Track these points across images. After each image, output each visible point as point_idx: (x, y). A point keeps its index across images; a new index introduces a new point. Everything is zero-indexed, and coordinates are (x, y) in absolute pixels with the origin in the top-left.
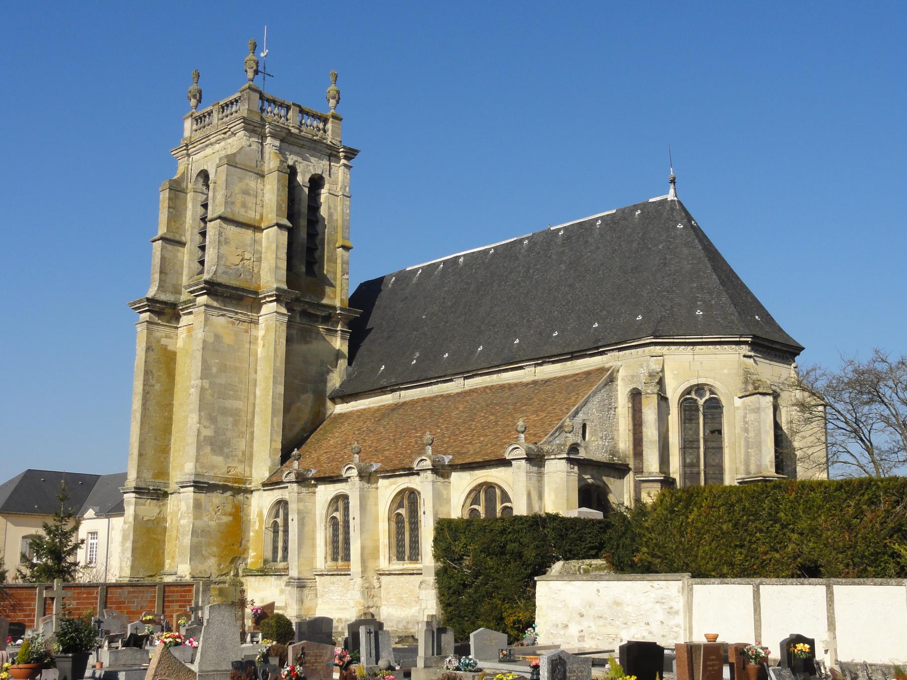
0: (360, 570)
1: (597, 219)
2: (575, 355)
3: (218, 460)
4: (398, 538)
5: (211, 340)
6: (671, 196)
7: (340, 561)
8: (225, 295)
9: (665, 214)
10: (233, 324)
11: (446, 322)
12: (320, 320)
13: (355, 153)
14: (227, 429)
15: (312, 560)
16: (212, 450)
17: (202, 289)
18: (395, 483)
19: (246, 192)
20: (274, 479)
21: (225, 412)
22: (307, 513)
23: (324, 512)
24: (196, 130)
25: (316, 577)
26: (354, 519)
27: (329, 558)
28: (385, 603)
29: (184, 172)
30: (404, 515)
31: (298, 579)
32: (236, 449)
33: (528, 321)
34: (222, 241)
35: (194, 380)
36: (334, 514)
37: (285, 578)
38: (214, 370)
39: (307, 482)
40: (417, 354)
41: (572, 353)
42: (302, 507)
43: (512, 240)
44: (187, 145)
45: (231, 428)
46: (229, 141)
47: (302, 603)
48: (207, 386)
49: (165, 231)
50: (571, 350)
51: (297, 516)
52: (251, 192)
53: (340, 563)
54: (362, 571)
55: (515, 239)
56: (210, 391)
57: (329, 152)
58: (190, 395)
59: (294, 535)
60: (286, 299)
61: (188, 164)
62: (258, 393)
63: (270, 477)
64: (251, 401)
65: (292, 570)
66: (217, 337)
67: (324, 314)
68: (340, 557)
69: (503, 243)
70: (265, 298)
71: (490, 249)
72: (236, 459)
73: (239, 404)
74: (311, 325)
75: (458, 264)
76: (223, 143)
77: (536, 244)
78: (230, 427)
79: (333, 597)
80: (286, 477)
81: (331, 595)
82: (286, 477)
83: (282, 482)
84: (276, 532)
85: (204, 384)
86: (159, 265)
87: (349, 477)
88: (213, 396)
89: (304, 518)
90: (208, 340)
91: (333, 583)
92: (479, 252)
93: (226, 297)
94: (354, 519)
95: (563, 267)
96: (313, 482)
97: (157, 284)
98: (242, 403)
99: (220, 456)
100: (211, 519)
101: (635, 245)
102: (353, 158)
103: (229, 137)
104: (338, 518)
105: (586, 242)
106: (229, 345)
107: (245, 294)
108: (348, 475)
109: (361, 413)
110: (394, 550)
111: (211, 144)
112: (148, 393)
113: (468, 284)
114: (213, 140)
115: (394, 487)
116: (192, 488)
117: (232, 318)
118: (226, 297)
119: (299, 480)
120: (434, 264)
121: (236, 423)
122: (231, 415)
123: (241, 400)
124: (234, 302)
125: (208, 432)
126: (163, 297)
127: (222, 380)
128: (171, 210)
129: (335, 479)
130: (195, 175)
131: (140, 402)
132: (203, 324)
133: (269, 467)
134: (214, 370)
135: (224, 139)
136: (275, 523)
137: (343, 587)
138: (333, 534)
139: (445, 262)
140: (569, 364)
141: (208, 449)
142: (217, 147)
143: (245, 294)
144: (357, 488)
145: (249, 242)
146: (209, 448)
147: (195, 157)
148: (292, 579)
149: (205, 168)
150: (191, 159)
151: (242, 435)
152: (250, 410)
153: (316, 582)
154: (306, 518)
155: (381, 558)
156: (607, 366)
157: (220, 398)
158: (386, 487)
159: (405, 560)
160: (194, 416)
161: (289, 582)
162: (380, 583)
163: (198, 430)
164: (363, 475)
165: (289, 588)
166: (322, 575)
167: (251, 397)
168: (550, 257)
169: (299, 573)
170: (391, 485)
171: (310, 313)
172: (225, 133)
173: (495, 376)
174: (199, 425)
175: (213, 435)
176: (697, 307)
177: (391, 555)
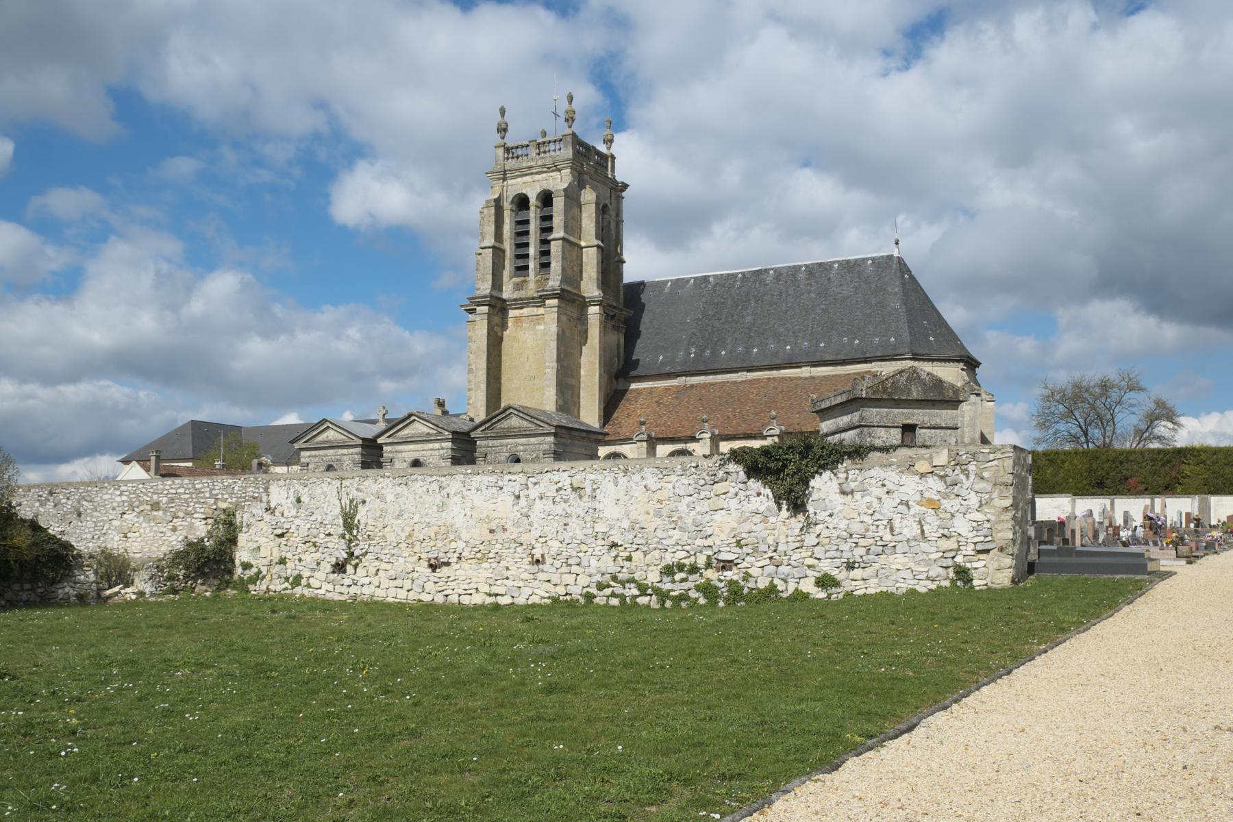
1: (834, 262)
2: (844, 362)
5: (560, 333)
6: (896, 254)
9: (894, 266)
10: (570, 320)
17: (557, 294)
19: (573, 218)
24: (508, 159)
33: (794, 333)
40: (693, 350)
41: (844, 360)
43: (758, 268)
44: (505, 171)
46: (551, 174)
49: (493, 241)
50: (843, 358)
55: (760, 268)
66: (563, 330)
69: (749, 270)
71: (738, 274)
75: (709, 281)
76: (544, 175)
77: (781, 274)
83: (632, 439)
86: (491, 268)
92: (728, 274)
95: (813, 295)
97: (490, 283)
101: (873, 286)
102: (624, 191)
103: (553, 171)
105: (829, 279)
108: (700, 437)
109: (651, 390)
111: (532, 174)
114: (534, 171)
120: (683, 279)
126: (495, 293)
130: (512, 197)
131: (485, 376)
132: (556, 320)
134: (562, 355)
135: (546, 172)
139: (696, 278)
140: (839, 367)
142: (537, 177)
145: (575, 257)
147: (510, 182)
149: (524, 192)
150: (505, 183)
156: (873, 370)
158: (724, 446)
168: (798, 286)
172: (548, 168)
173: (775, 372)
176: (930, 335)
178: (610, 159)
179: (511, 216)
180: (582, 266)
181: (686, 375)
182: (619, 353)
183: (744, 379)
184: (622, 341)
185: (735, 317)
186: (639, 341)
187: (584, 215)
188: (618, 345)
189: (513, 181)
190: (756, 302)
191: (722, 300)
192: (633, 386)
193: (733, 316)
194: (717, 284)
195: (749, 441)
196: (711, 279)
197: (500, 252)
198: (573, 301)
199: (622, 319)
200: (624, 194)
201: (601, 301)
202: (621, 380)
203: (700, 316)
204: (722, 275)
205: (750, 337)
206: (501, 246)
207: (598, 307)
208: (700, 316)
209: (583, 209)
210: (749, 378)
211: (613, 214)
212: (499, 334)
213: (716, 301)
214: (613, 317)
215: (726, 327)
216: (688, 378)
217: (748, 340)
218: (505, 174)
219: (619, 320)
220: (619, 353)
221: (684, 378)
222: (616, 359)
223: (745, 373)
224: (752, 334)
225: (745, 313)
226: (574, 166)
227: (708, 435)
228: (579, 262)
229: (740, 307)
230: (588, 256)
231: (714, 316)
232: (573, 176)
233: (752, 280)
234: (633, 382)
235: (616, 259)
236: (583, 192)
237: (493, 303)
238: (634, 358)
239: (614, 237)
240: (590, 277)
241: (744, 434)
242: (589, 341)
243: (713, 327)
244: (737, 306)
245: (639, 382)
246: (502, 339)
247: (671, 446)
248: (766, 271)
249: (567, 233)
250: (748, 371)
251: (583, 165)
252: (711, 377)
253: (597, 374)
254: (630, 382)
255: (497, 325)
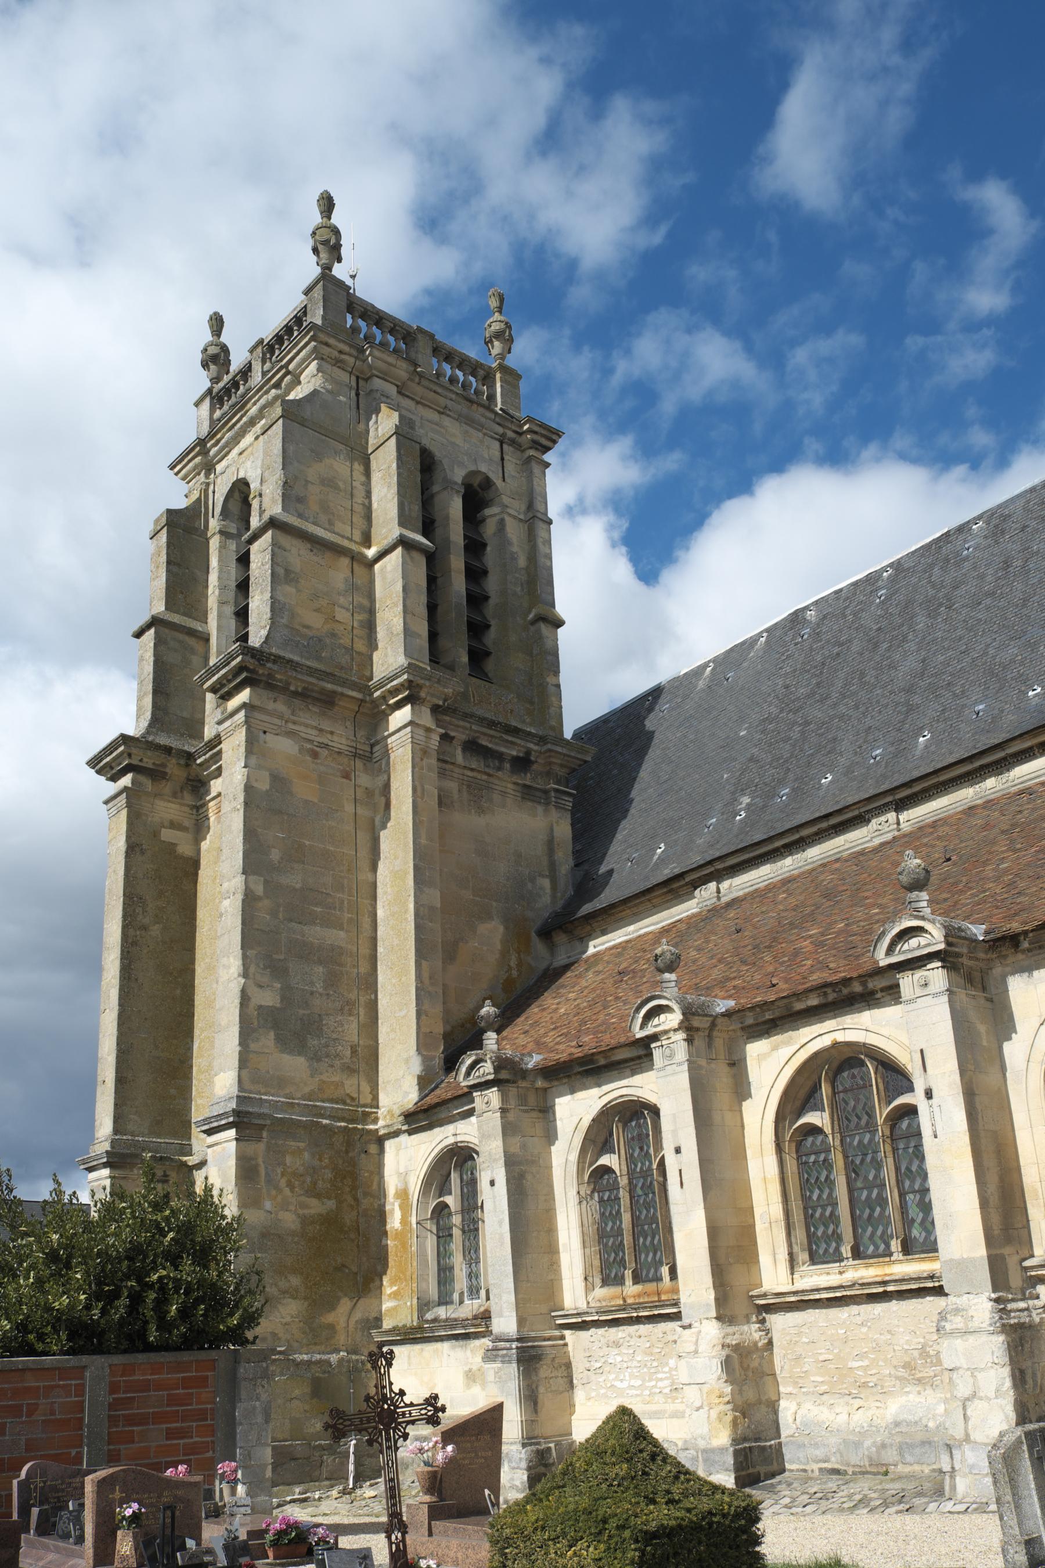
0: (712, 1295)
3: (295, 1065)
4: (806, 1200)
7: (629, 1281)
8: (292, 688)
10: (315, 755)
11: (807, 723)
12: (507, 766)
13: (554, 437)
14: (312, 993)
15: (551, 1289)
16: (278, 1039)
17: (241, 669)
18: (788, 1043)
20: (431, 1100)
21: (306, 952)
22: (533, 1162)
23: (574, 1156)
25: (567, 1333)
26: (678, 1151)
27: (598, 1281)
28: (789, 1389)
29: (199, 499)
30: (828, 1130)
31: (518, 1340)
32: (335, 1040)
34: (281, 575)
35: (229, 880)
36: (605, 1160)
37: (486, 1342)
38: (275, 855)
39: (523, 1084)
40: (746, 800)
42: (515, 1149)
45: (321, 990)
47: (536, 1403)
48: (259, 889)
49: (163, 608)
51: (503, 1170)
52: (341, 484)
53: (631, 1289)
54: (717, 1299)
56: (266, 903)
57: (500, 430)
58: (221, 915)
59: (500, 1223)
60: (433, 695)
61: (208, 484)
62: (380, 913)
63: (421, 1100)
64: (366, 932)
65: (501, 1315)
66: (277, 779)
67: (514, 753)
68: (628, 1274)
70: (383, 698)
72: (337, 1063)
73: (337, 937)
74: (489, 775)
78: (319, 987)
79: (618, 1384)
80: (468, 1074)
81: (612, 1377)
82: (468, 1074)
84: (444, 1236)
85: (252, 886)
87: (655, 1037)
88: (274, 914)
89: (522, 1176)
90: (255, 784)
91: (617, 1345)
93: (296, 694)
94: (678, 1151)
96: (540, 1083)
98: (342, 934)
99: (299, 1054)
100: (284, 1206)
102: (548, 449)
104: (616, 1167)
106: (306, 802)
107: (339, 689)
110: (800, 1234)
112: (134, 943)
113: (841, 645)
115: (786, 1052)
116: (232, 1133)
117: (311, 741)
118: (296, 694)
119: (504, 1075)
121: (333, 980)
122: (320, 962)
123: (342, 929)
124: (315, 709)
125: (268, 998)
127: (294, 880)
128: (175, 569)
129: (602, 1062)
130: (222, 499)
133: (419, 1078)
134: (275, 855)
136: (441, 1209)
137: (648, 1352)
138: (602, 1215)
141: (267, 1041)
143: (339, 689)
144: (680, 1064)
146: (272, 1034)
148: (501, 1340)
149: (241, 475)
151: (348, 1007)
152: (364, 950)
153: (566, 1345)
154: (529, 1177)
155: (765, 1258)
157: (291, 920)
158: (761, 1058)
159: (841, 1260)
160: (232, 960)
161: (495, 1349)
162: (768, 1331)
163: (243, 991)
164: (696, 1022)
165: (492, 1367)
166: (583, 1326)
167: (366, 921)
169: (521, 1322)
170: (775, 1048)
171: (483, 746)
174: (243, 981)
175: (278, 1005)
177: (796, 1249)
178: (498, 376)
179: (222, 547)
180: (372, 612)
181: (718, 876)
182: (553, 866)
183: (889, 837)
184: (564, 829)
185: (869, 678)
186: (624, 824)
187: (376, 477)
188: (550, 844)
189: (224, 463)
190: (933, 614)
191: (836, 650)
192: (596, 946)
193: (863, 675)
194: (825, 617)
195: (848, 1020)
196: (811, 615)
197: (191, 641)
198: (327, 701)
199: (562, 772)
200: (548, 457)
201: (409, 684)
202: (560, 938)
203: (774, 710)
204: (841, 590)
205: (911, 709)
206: (198, 626)
207: (408, 708)
208: (774, 710)
209: (374, 465)
210: (905, 827)
211: (516, 507)
212: (185, 849)
213: (819, 658)
214: (522, 763)
215: (842, 709)
216: (725, 885)
217: (903, 722)
218: (205, 452)
219: (548, 774)
220: (553, 866)
221: (713, 885)
222: (546, 883)
223: (891, 816)
224: (916, 699)
225: (897, 657)
226: (326, 350)
227: (671, 1020)
228: (366, 602)
229: (885, 646)
230: (384, 578)
231: (811, 695)
232: (329, 378)
233: (920, 568)
234: (590, 936)
235: (531, 616)
236: (371, 423)
237: (148, 763)
238: (603, 869)
239: (522, 562)
240: (390, 633)
241: (822, 987)
242: (393, 814)
243: (807, 723)
244: (876, 646)
245: (604, 933)
246: (195, 864)
247: (595, 1092)
248: (962, 529)
249: (300, 516)
250: (900, 806)
251: (363, 351)
252: (788, 861)
253: (411, 906)
254: (584, 940)
255: (173, 825)
